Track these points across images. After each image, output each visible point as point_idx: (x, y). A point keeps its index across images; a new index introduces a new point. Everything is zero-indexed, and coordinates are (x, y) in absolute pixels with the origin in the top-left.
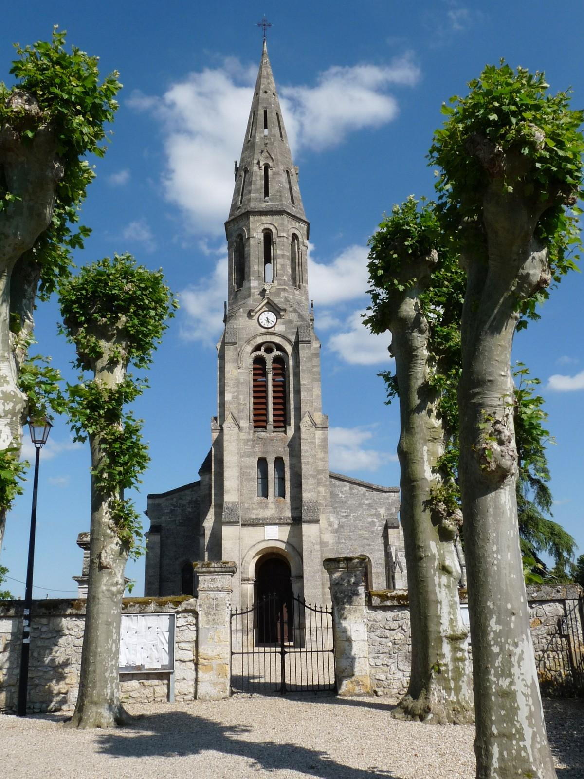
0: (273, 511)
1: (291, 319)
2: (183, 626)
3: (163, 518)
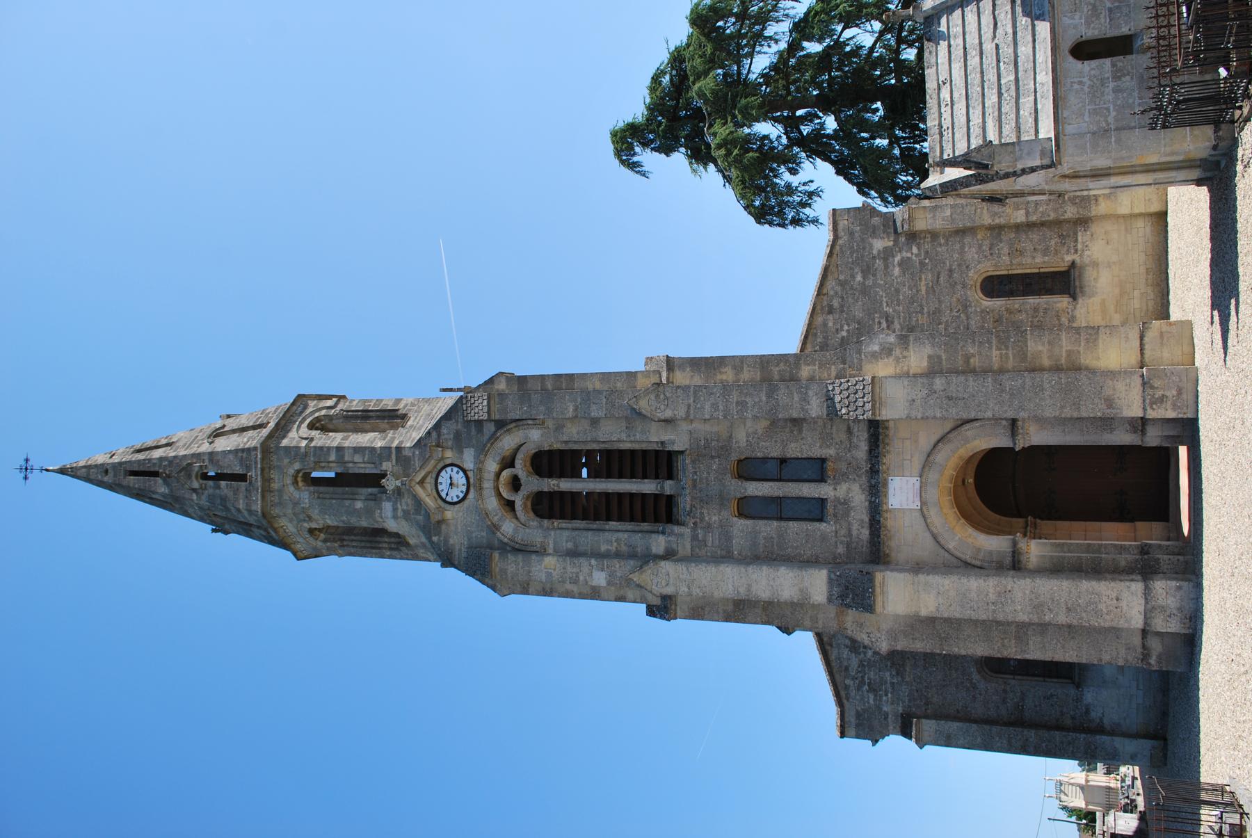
0: (856, 488)
1: (452, 436)
2: (1172, 821)
3: (885, 709)
